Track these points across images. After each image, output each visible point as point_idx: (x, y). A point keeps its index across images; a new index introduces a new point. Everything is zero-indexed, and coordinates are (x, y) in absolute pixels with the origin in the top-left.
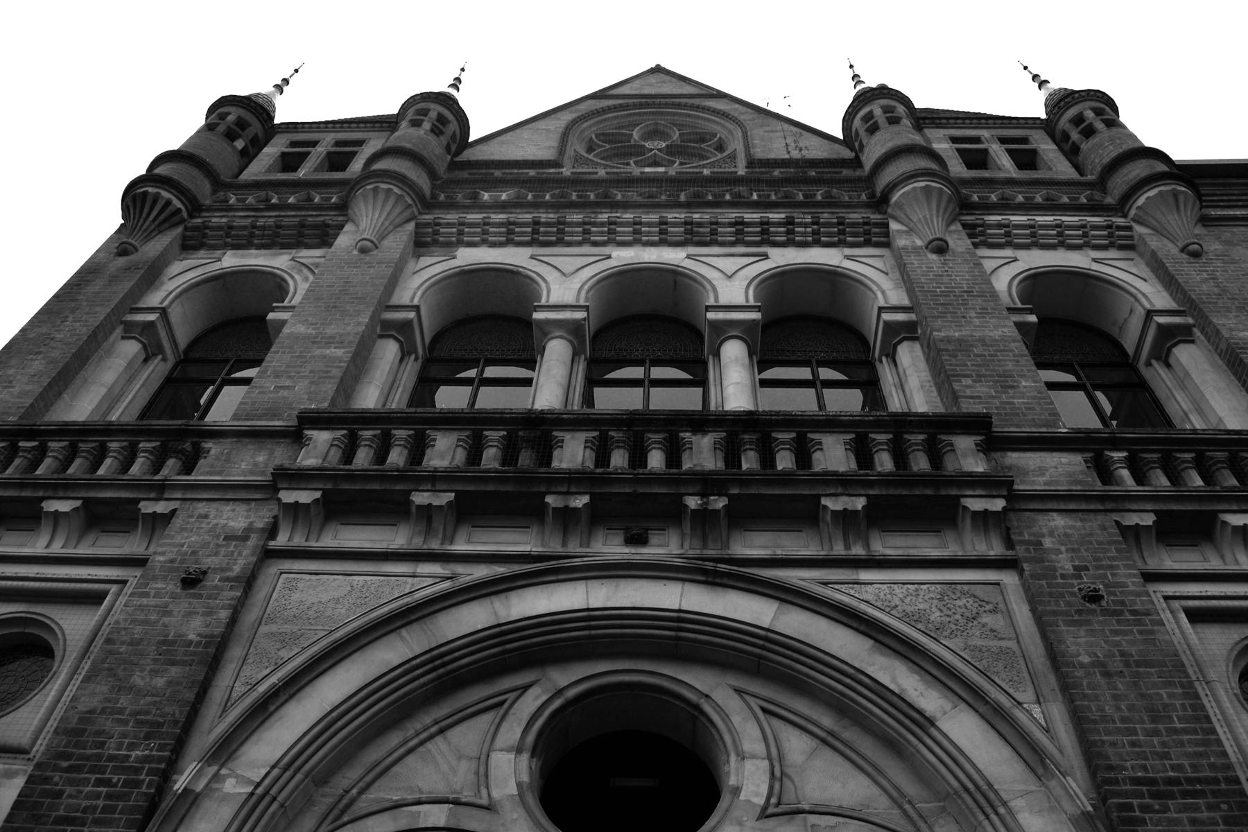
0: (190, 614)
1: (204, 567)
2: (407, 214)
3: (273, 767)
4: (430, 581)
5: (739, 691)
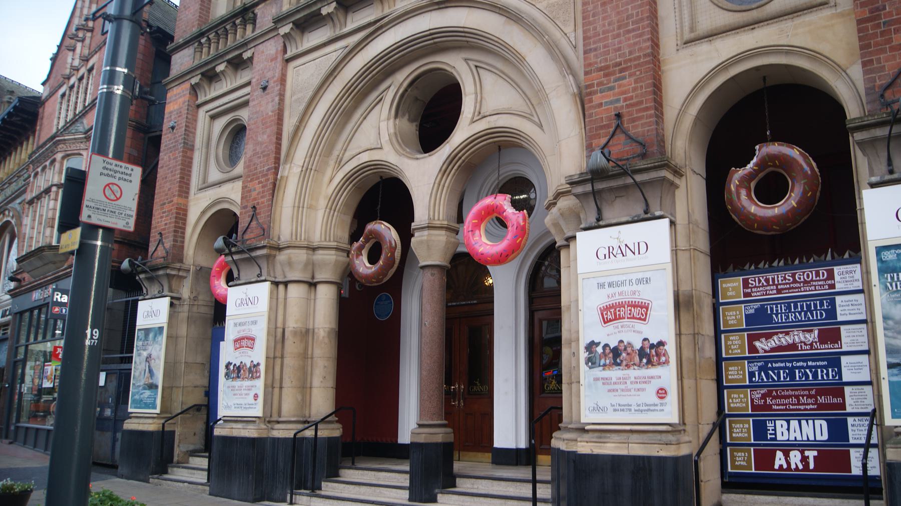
0: (267, 103)
1: (266, 79)
3: (306, 158)
4: (341, 51)
5: (466, 60)
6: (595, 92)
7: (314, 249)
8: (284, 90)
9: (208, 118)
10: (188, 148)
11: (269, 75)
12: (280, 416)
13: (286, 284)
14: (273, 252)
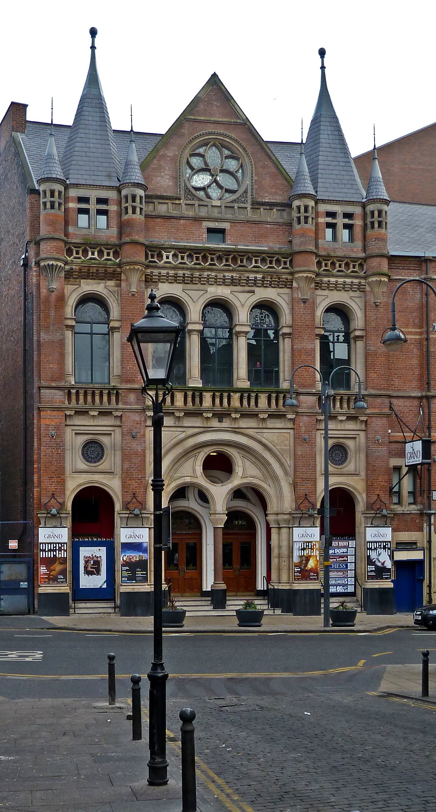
6: (299, 485)
11: (135, 431)
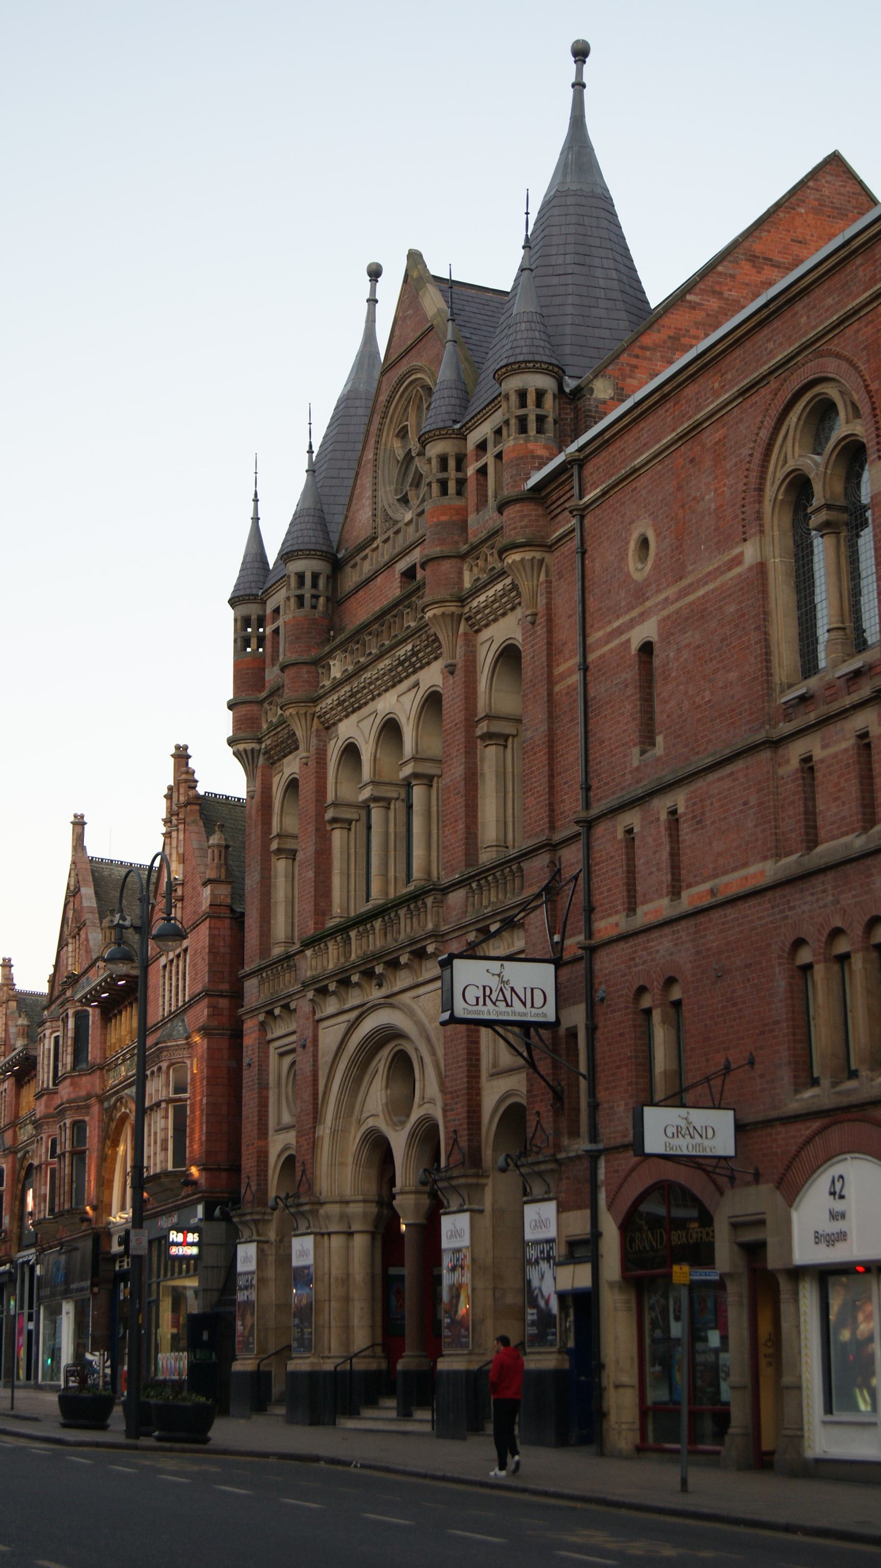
2: (309, 717)
7: (347, 1203)
8: (317, 1051)
9: (276, 1056)
10: (263, 1087)
12: (330, 1351)
13: (329, 1234)
14: (317, 1207)
